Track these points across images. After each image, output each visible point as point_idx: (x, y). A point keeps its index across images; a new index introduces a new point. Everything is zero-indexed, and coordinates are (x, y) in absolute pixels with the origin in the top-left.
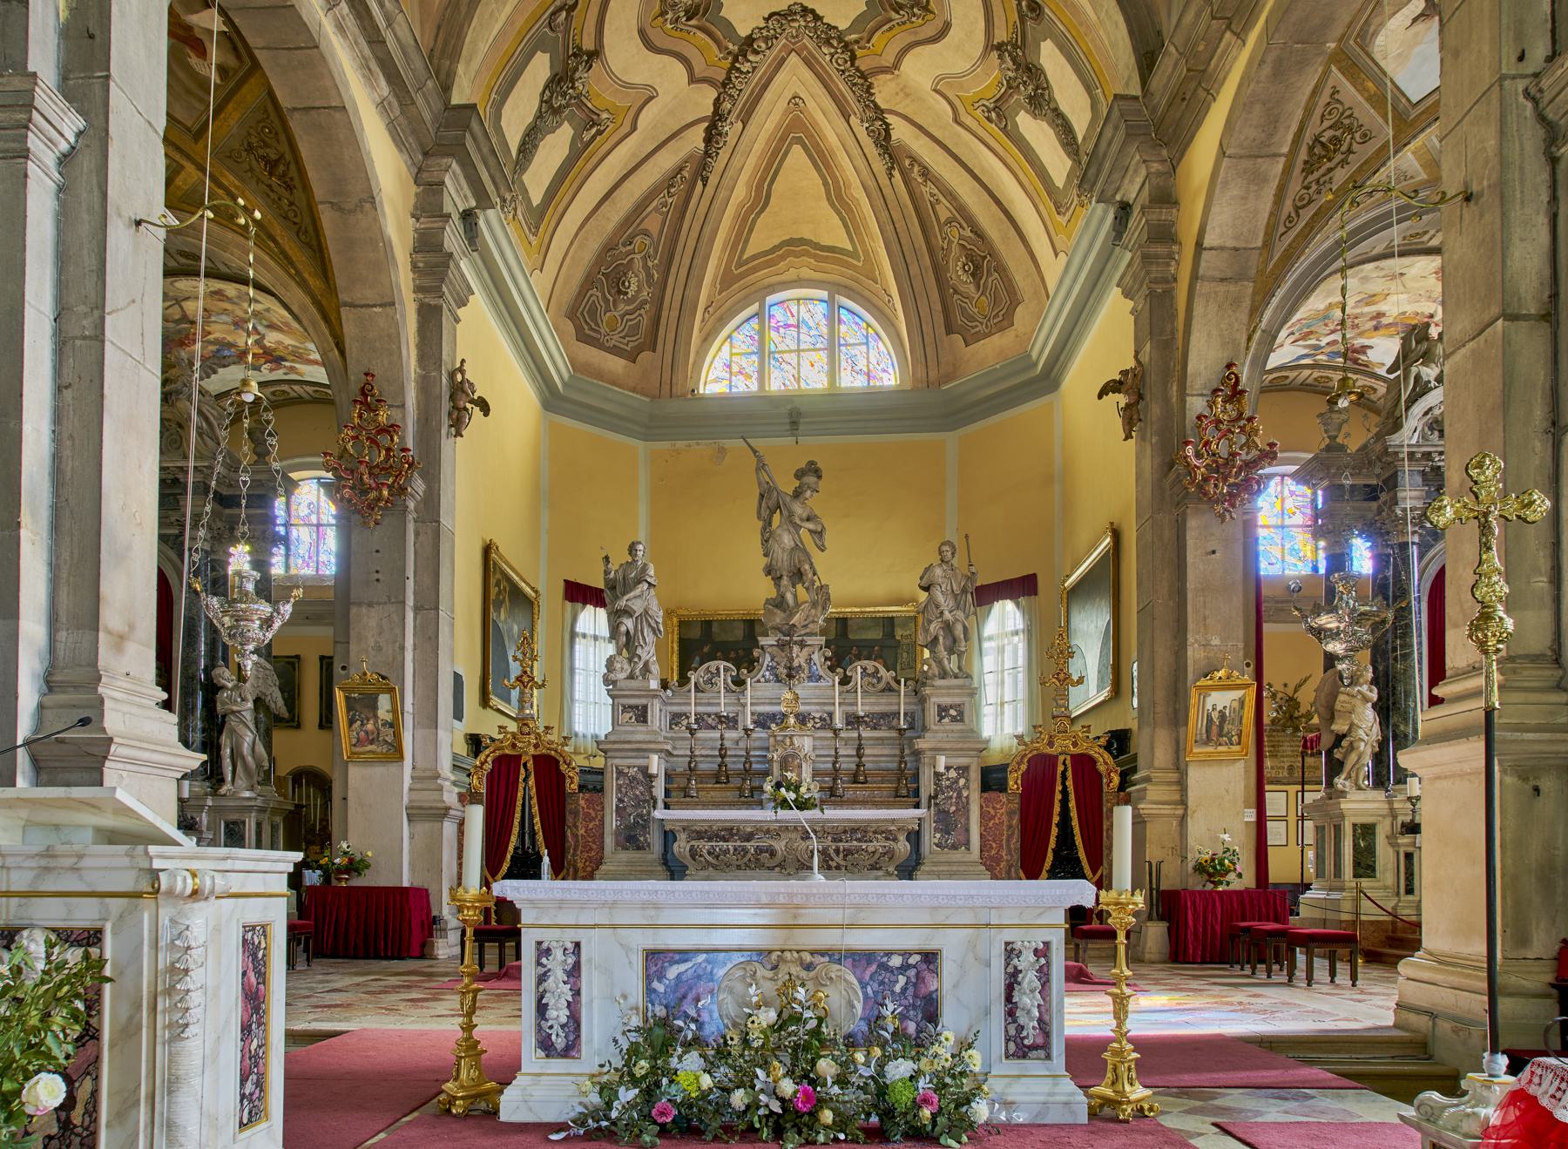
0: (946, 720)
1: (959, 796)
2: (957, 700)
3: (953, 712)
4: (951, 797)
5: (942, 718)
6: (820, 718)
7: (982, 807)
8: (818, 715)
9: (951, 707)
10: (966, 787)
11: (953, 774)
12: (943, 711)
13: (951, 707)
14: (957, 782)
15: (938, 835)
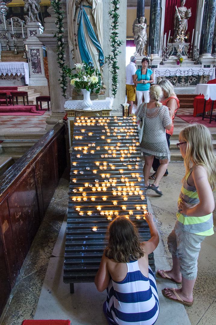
0: (32, 35)
1: (38, 58)
2: (35, 29)
3: (34, 33)
4: (35, 59)
5: (31, 35)
6: (3, 35)
7: (44, 61)
8: (3, 34)
9: (34, 31)
10: (39, 55)
11: (35, 51)
12: (31, 32)
13: (33, 31)
14: (36, 54)
15: (33, 69)
